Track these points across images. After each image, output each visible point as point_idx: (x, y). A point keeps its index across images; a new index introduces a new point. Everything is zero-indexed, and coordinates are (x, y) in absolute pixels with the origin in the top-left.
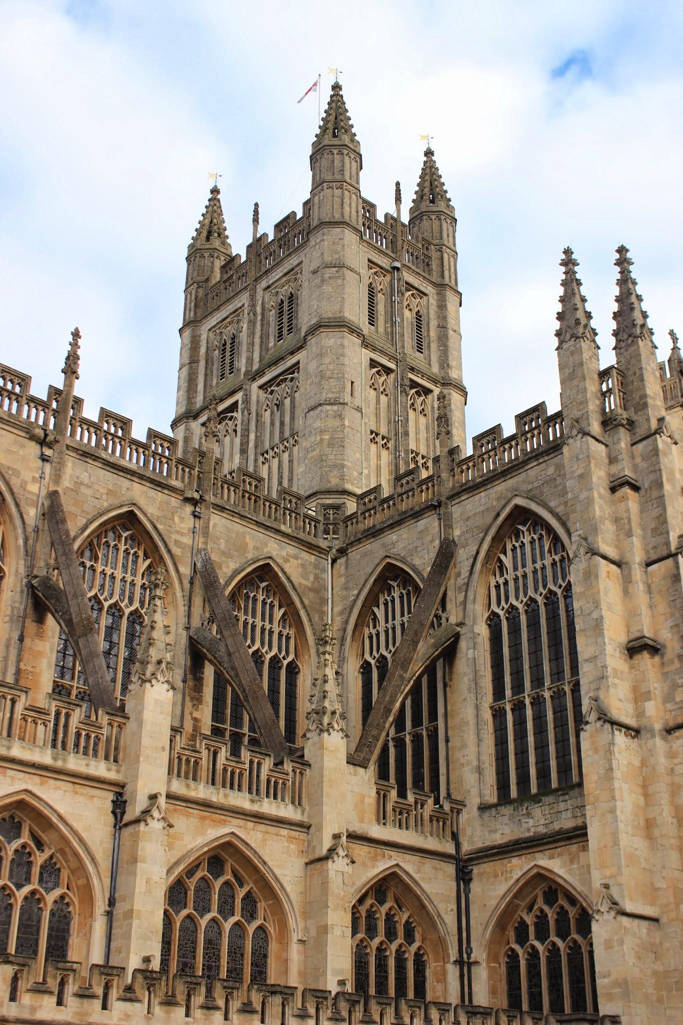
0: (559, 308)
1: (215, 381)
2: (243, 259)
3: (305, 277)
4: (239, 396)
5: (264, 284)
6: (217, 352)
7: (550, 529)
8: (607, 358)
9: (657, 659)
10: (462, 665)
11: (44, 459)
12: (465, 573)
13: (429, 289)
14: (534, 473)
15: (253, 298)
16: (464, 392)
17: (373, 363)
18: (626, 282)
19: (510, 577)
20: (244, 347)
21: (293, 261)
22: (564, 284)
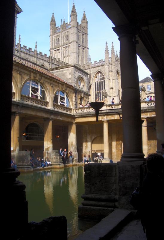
0: (105, 49)
1: (56, 44)
2: (60, 27)
3: (70, 33)
4: (60, 48)
5: (63, 32)
6: (56, 40)
7: (102, 74)
8: (110, 56)
9: (113, 89)
10: (92, 87)
11: (50, 65)
12: (92, 77)
13: (84, 34)
14: (101, 67)
15: (62, 34)
16: (88, 49)
17: (79, 46)
18: (113, 46)
19: (97, 78)
20: (61, 41)
21: (68, 30)
22: (106, 46)
